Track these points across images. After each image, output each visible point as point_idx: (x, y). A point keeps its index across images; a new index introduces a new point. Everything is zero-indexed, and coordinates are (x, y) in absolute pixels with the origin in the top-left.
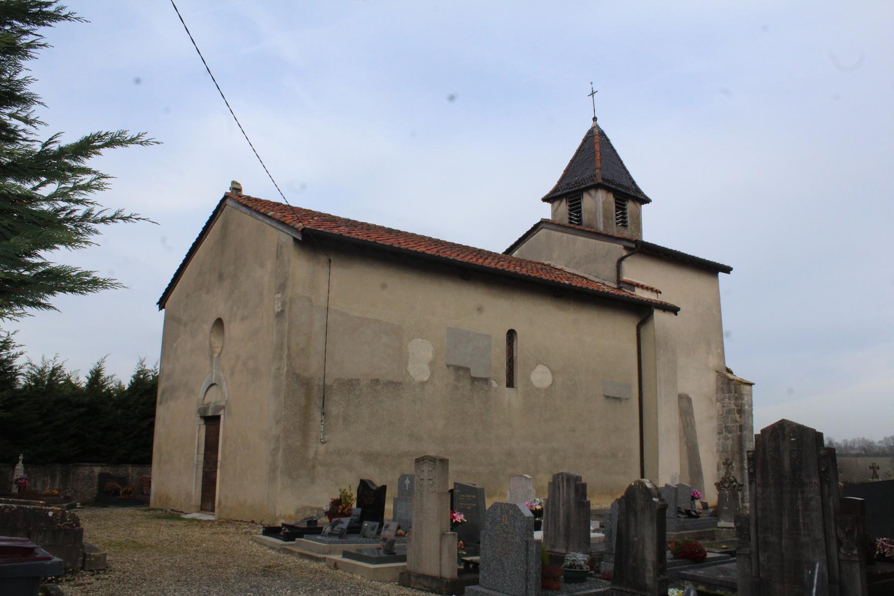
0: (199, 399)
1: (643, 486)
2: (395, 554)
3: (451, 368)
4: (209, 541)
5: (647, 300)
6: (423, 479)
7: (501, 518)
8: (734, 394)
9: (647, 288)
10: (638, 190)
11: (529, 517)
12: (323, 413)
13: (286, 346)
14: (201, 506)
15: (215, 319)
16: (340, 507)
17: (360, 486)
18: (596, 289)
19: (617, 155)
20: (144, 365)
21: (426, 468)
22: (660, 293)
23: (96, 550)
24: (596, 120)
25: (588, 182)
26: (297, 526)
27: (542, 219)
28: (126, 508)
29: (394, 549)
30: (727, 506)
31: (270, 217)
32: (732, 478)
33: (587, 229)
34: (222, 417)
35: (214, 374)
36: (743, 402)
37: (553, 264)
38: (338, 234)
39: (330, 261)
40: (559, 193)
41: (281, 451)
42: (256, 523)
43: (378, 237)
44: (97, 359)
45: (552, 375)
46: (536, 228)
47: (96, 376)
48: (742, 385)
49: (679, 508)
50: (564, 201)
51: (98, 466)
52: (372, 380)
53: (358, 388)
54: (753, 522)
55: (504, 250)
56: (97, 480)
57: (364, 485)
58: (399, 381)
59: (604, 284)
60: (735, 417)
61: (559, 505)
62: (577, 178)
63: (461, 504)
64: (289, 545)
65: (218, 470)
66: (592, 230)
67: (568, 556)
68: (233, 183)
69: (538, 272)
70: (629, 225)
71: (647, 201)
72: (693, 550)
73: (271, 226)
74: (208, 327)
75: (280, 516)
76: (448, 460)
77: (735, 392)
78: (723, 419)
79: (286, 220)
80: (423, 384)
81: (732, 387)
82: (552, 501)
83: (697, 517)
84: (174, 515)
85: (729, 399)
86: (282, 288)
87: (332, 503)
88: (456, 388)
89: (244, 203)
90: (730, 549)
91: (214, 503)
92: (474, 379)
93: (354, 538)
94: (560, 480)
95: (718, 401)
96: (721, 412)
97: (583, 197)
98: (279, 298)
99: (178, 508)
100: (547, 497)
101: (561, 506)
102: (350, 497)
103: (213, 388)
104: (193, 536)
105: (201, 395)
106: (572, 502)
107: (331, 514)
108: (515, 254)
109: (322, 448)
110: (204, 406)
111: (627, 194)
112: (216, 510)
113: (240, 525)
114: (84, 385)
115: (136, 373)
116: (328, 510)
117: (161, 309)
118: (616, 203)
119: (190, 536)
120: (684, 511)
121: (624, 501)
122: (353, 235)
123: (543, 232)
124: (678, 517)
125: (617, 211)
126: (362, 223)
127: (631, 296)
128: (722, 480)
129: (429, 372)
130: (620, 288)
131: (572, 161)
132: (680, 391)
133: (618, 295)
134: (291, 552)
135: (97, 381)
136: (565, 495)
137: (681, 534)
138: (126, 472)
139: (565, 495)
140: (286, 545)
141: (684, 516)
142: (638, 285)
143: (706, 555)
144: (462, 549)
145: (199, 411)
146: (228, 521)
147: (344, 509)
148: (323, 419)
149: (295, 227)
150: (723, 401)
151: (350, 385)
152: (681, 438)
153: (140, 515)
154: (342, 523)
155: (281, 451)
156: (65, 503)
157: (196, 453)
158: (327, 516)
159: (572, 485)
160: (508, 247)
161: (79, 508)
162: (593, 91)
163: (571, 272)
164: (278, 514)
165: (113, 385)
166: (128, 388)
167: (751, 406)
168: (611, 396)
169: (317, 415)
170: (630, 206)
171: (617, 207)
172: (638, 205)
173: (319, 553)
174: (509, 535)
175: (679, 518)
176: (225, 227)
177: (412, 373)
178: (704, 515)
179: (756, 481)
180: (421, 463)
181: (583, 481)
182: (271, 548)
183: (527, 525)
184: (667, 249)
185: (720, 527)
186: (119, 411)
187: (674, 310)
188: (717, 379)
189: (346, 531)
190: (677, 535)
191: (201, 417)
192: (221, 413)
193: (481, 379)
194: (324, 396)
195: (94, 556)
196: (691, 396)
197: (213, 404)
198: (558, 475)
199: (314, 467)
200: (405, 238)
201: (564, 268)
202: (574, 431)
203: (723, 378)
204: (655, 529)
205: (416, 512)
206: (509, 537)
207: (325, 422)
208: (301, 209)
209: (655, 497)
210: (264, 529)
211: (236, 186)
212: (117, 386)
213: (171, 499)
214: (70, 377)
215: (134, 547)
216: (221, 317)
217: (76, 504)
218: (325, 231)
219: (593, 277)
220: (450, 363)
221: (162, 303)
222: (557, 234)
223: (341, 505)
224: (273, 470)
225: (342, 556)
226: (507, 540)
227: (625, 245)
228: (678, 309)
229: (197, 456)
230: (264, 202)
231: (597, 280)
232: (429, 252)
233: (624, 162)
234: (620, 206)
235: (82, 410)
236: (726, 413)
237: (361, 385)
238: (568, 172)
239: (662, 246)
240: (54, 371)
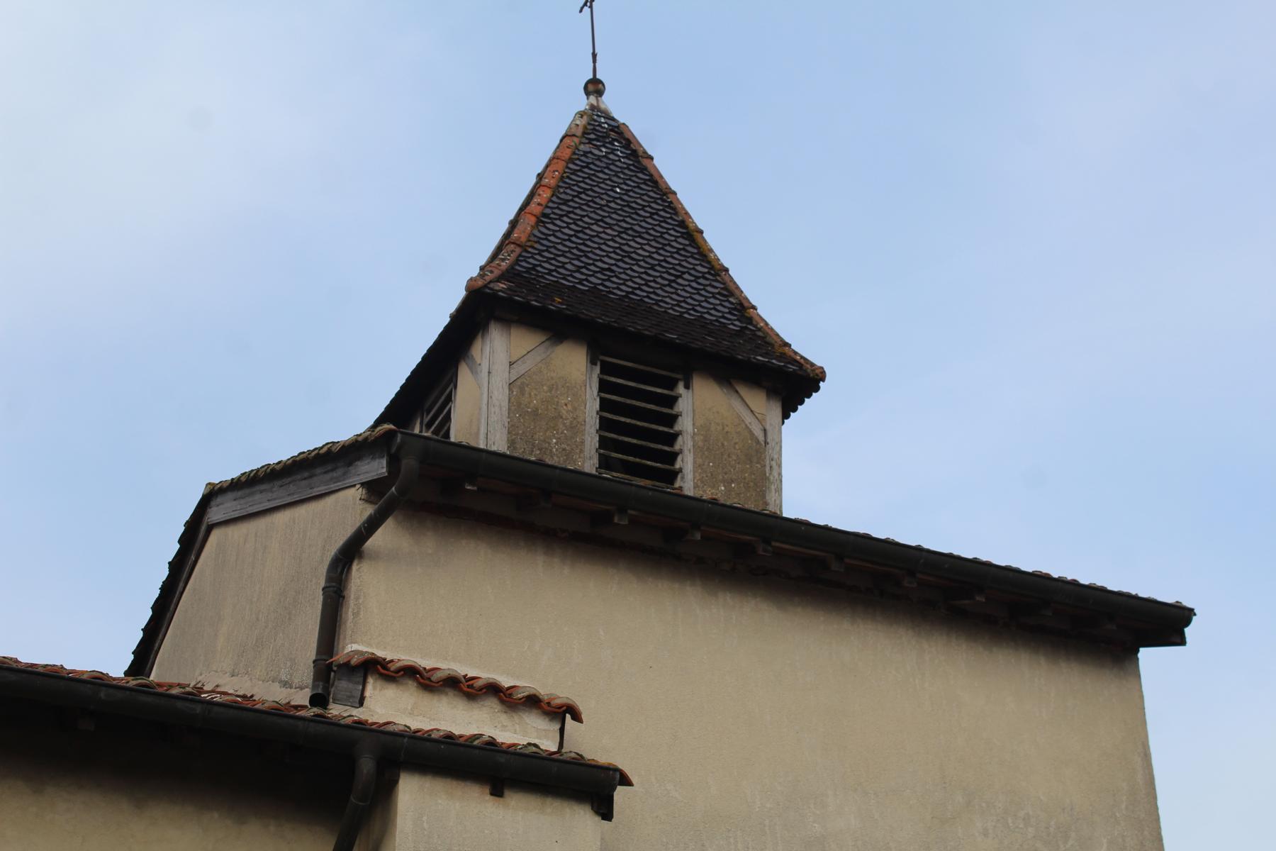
118: (604, 386)
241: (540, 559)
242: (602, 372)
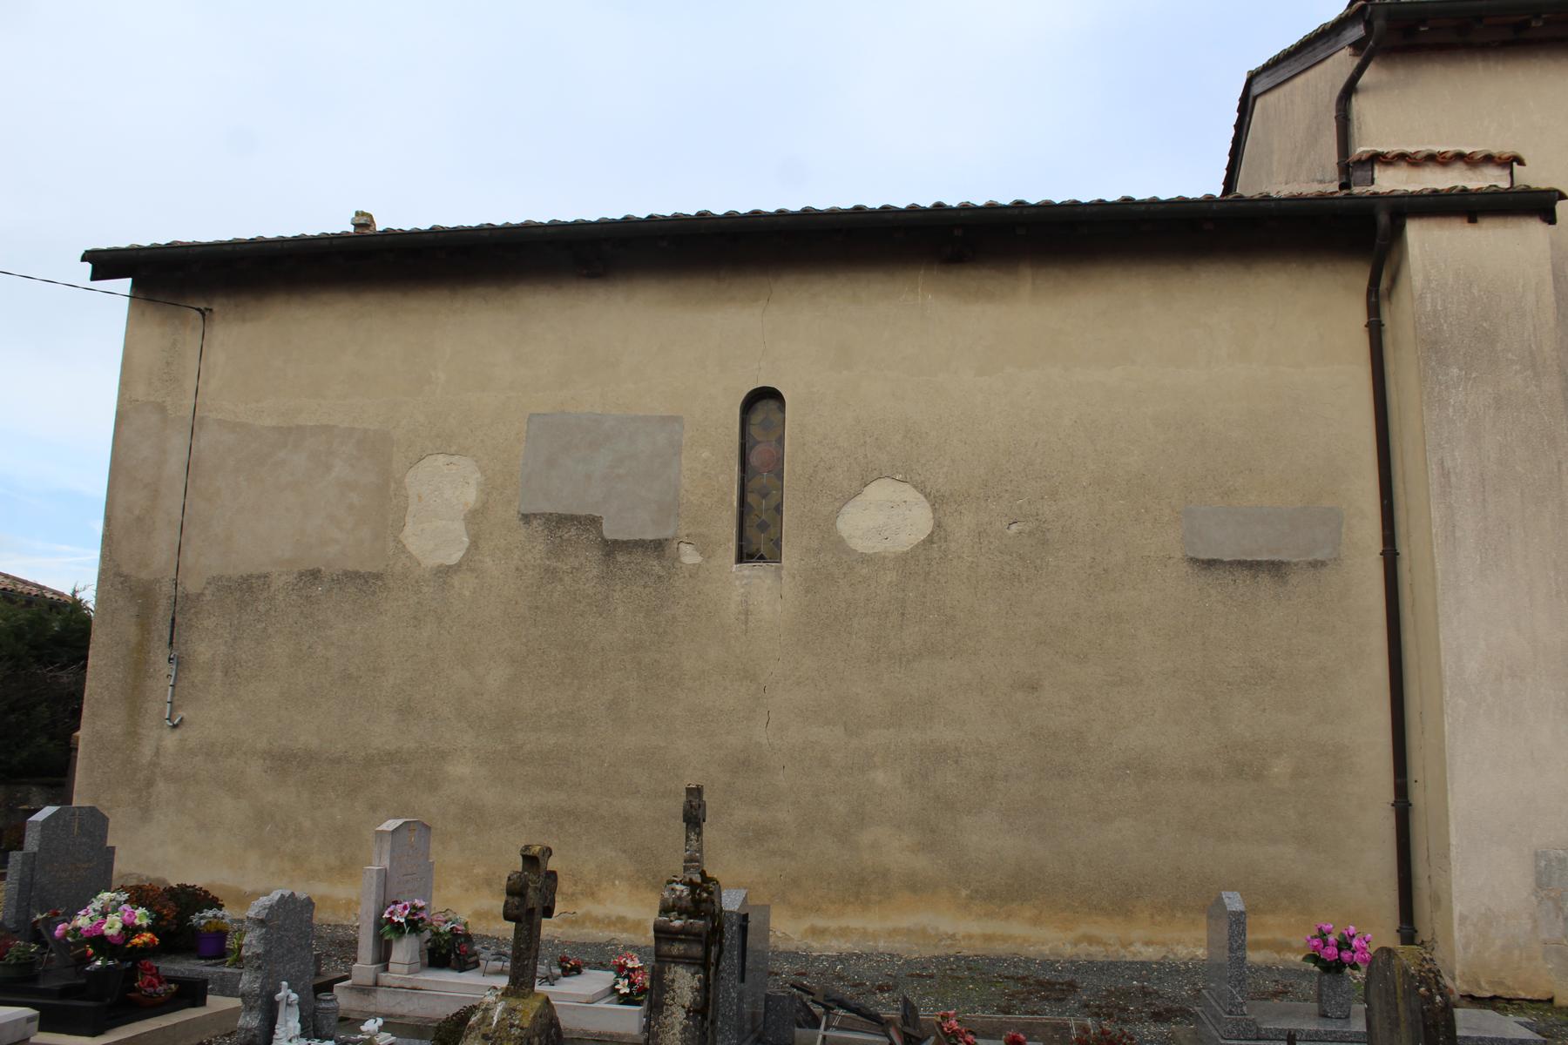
3: (535, 523)
45: (934, 510)
46: (1246, 106)
52: (301, 575)
53: (265, 594)
80: (445, 572)
88: (552, 574)
92: (612, 548)
109: (171, 740)
129: (466, 539)
177: (412, 548)
193: (640, 544)
199: (150, 783)
202: (1033, 687)
237: (272, 589)
241: (1480, 65)
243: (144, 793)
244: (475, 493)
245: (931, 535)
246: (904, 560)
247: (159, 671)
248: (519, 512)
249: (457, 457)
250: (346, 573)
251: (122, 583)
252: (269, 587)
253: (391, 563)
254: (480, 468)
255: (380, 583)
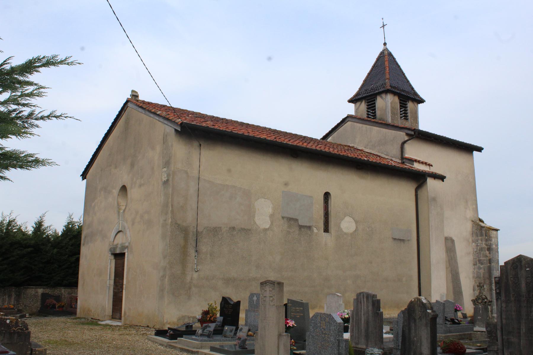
0: (110, 242)
1: (420, 301)
2: (247, 348)
3: (285, 219)
4: (118, 340)
5: (422, 171)
6: (266, 297)
7: (321, 323)
8: (485, 237)
9: (422, 163)
10: (416, 94)
11: (340, 323)
12: (197, 251)
13: (170, 204)
14: (112, 316)
15: (121, 186)
16: (208, 316)
17: (222, 301)
18: (386, 163)
19: (401, 69)
20: (72, 218)
21: (268, 288)
22: (432, 166)
23: (40, 346)
24: (386, 45)
25: (380, 88)
26: (178, 329)
27: (348, 115)
28: (60, 317)
29: (246, 345)
30: (480, 316)
31: (158, 115)
32: (484, 297)
33: (380, 122)
34: (126, 254)
35: (121, 224)
36: (491, 242)
37: (356, 146)
38: (206, 126)
39: (200, 145)
40: (360, 96)
41: (167, 277)
42: (150, 328)
43: (234, 128)
44: (40, 214)
45: (356, 224)
46: (344, 121)
47: (39, 225)
48: (490, 231)
49: (446, 317)
50: (364, 102)
51: (41, 288)
52: (230, 228)
54: (499, 327)
55: (322, 137)
56: (40, 298)
57: (225, 301)
58: (249, 228)
59: (392, 160)
60: (486, 253)
61: (361, 315)
62: (372, 86)
63: (292, 314)
64: (173, 342)
65: (124, 291)
66: (383, 122)
67: (367, 351)
68: (133, 91)
69: (345, 152)
70: (409, 118)
71: (422, 101)
72: (456, 347)
73: (159, 121)
74: (116, 191)
75: (167, 322)
76: (283, 283)
77: (486, 236)
78: (477, 255)
79: (169, 117)
80: (266, 230)
81: (484, 232)
82: (356, 311)
83: (459, 324)
84: (94, 322)
85: (482, 241)
86: (167, 164)
87: (203, 313)
89: (140, 105)
90: (482, 346)
91: (121, 314)
92: (301, 227)
93: (218, 337)
94: (362, 297)
95: (473, 242)
96: (475, 250)
97: (377, 99)
98: (165, 171)
99: (96, 317)
100: (353, 309)
101: (362, 315)
102: (215, 309)
103: (120, 235)
104: (107, 337)
105: (112, 239)
106: (370, 313)
107: (202, 321)
108: (330, 139)
109: (195, 275)
110: (114, 246)
111: (408, 96)
112: (123, 318)
113: (139, 328)
114: (30, 233)
115: (66, 224)
116: (200, 318)
117: (83, 179)
118: (400, 103)
119: (104, 337)
120: (449, 320)
121: (406, 312)
122: (216, 127)
123: (348, 124)
124: (446, 323)
125: (401, 109)
126: (223, 119)
127: (411, 168)
128: (477, 298)
130: (403, 163)
131: (369, 74)
132: (446, 235)
133: (402, 168)
134: (174, 348)
135: (40, 229)
136: (365, 307)
137: (448, 336)
138: (60, 292)
139: (365, 307)
140: (171, 342)
141: (450, 323)
142: (416, 161)
143: (465, 351)
144: (293, 345)
145: (110, 250)
146: (131, 326)
147: (211, 317)
148: (196, 255)
149: (176, 122)
150: (477, 242)
151: (215, 231)
152: (447, 268)
153: (69, 322)
154: (210, 327)
155: (167, 277)
156: (18, 314)
157: (108, 278)
158: (199, 323)
159: (370, 301)
160: (324, 134)
161: (28, 317)
162: (383, 24)
163: (369, 152)
164: (165, 321)
165: (50, 232)
166: (61, 234)
167: (497, 245)
168: (397, 238)
169: (192, 252)
170: (410, 105)
171: (400, 106)
172: (416, 104)
173: (194, 348)
174: (326, 336)
175: (446, 325)
176: (127, 122)
178: (464, 322)
179: (501, 299)
180: (264, 285)
181: (378, 298)
182: (161, 345)
183: (339, 329)
184: (436, 135)
185: (475, 331)
186: (55, 250)
187: (442, 178)
188: (473, 227)
189: (212, 333)
190: (445, 336)
191: (112, 254)
192: (126, 251)
193: (306, 227)
194: (197, 239)
195: (38, 351)
196: (454, 238)
197: (120, 245)
198: (360, 293)
199: (190, 288)
200: (252, 129)
201: (364, 149)
203: (477, 226)
204: (429, 332)
205: (261, 320)
206: (326, 337)
207: (197, 257)
208: (180, 109)
209: (429, 309)
210: (156, 331)
211: (135, 94)
212: (54, 233)
213: (91, 311)
214: (21, 227)
215: (66, 344)
216: (125, 185)
217: (25, 315)
218: (197, 124)
219: (384, 155)
220: (284, 216)
221: (84, 175)
222: (359, 125)
223: (209, 314)
224: (162, 290)
225: (210, 350)
226: (325, 339)
227: (407, 132)
228: (445, 177)
229: (109, 282)
230: (154, 105)
231: (387, 157)
232: (269, 139)
233: (405, 74)
234: (403, 106)
235: (30, 249)
236: (479, 251)
237: (222, 231)
238: (365, 81)
239: (433, 133)
240: (10, 223)
242: (400, 100)
243: (189, 291)
244: (271, 210)
245: (356, 229)
246: (352, 234)
247: (191, 254)
248: (281, 216)
249: (267, 200)
250: (242, 229)
251: (178, 226)
252: (221, 231)
253: (253, 227)
254: (272, 203)
255: (250, 232)
